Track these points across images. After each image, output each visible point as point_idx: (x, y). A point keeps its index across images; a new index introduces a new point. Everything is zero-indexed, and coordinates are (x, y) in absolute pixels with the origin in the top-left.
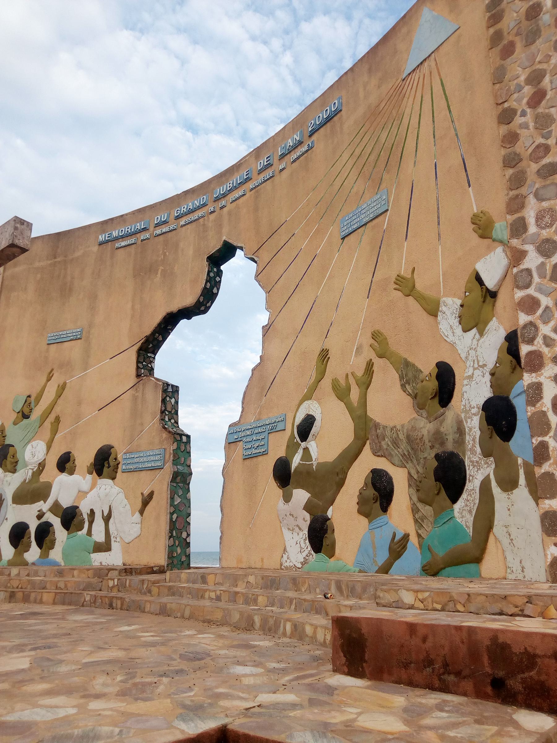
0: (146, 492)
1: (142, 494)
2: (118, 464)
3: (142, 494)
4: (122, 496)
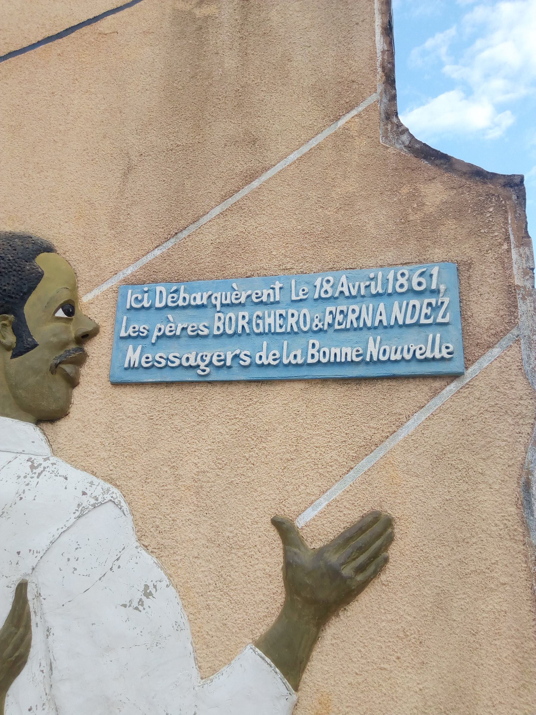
0: (321, 520)
1: (283, 528)
2: (86, 337)
3: (283, 528)
4: (112, 526)
